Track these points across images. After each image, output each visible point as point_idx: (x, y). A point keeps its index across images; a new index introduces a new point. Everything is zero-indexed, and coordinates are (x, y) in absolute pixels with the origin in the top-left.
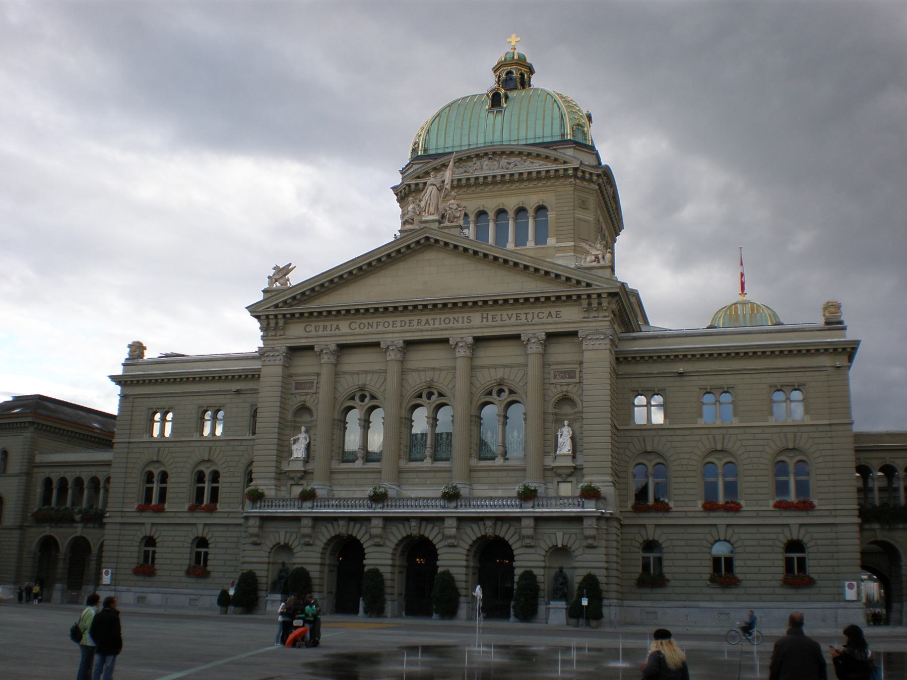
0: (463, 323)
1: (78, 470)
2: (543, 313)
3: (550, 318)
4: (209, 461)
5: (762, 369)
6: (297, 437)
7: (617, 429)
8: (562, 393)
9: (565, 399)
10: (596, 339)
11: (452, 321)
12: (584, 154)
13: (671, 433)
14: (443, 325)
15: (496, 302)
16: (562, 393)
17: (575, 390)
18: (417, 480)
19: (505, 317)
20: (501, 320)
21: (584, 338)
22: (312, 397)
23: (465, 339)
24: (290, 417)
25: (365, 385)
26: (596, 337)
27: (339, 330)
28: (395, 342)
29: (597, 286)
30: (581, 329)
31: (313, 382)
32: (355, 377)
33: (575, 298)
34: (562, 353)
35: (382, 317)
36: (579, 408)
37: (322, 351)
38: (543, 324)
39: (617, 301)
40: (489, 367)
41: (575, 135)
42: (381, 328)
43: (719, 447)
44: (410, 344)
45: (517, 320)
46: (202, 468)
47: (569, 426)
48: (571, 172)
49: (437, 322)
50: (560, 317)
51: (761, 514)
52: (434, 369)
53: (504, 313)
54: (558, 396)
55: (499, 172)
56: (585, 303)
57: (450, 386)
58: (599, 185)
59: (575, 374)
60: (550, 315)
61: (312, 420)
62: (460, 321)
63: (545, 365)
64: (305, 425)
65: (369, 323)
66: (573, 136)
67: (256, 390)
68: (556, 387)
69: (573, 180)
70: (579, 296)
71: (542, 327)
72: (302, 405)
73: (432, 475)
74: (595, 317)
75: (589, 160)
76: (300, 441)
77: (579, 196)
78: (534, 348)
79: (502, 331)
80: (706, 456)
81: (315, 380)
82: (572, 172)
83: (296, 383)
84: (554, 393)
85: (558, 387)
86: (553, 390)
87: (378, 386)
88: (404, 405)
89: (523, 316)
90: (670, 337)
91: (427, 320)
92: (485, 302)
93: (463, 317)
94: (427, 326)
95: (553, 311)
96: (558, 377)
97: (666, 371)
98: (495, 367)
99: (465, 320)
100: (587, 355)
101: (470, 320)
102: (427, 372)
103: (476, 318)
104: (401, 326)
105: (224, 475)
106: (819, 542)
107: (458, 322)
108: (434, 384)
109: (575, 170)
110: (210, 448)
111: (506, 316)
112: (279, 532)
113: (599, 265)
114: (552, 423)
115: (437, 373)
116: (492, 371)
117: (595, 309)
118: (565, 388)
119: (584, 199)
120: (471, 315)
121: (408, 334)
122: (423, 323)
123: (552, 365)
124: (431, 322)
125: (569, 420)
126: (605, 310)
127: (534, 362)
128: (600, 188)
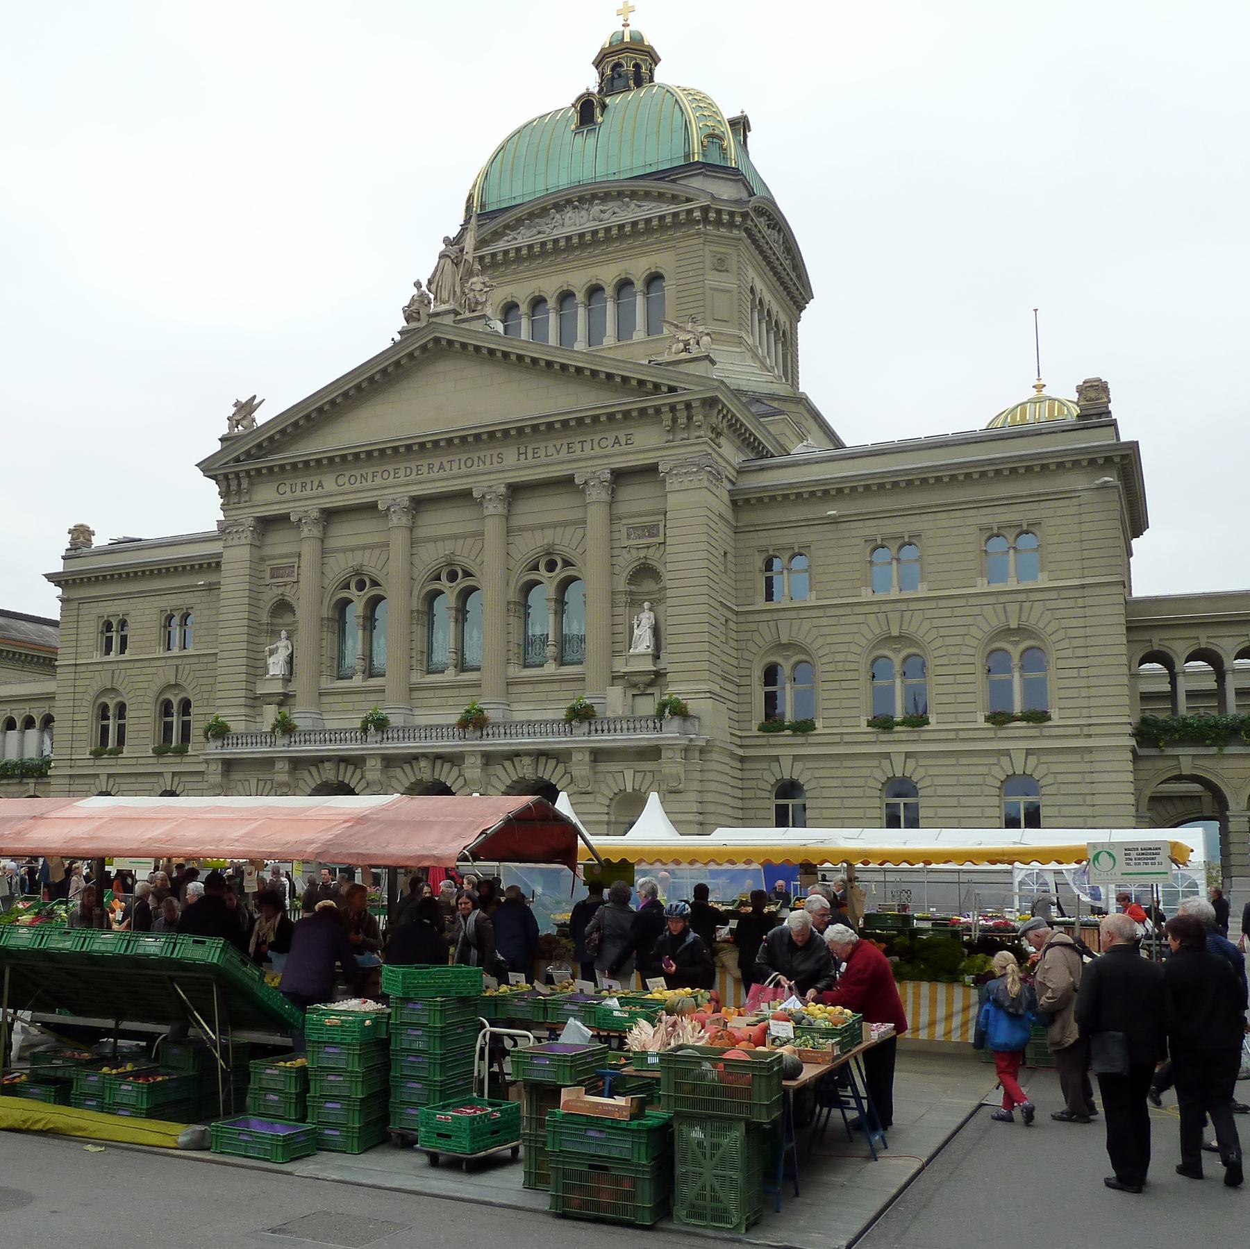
0: (492, 464)
1: (26, 706)
4: (176, 685)
5: (963, 503)
6: (275, 646)
7: (737, 613)
8: (638, 560)
9: (645, 572)
10: (685, 473)
11: (476, 463)
12: (721, 183)
13: (820, 613)
14: (464, 469)
15: (535, 428)
16: (638, 560)
17: (658, 555)
19: (551, 451)
21: (667, 473)
24: (265, 618)
25: (362, 566)
26: (685, 471)
28: (398, 500)
30: (661, 459)
32: (349, 555)
33: (651, 411)
34: (636, 498)
37: (300, 520)
38: (606, 456)
39: (719, 412)
40: (533, 528)
41: (707, 153)
42: (378, 481)
43: (895, 633)
44: (419, 503)
46: (168, 696)
48: (697, 214)
49: (455, 466)
51: (962, 735)
52: (455, 537)
53: (550, 444)
54: (633, 565)
55: (592, 225)
56: (667, 418)
57: (478, 560)
58: (747, 230)
60: (617, 441)
62: (488, 460)
63: (613, 519)
64: (287, 629)
66: (704, 155)
67: (215, 584)
68: (629, 551)
69: (701, 226)
70: (658, 410)
71: (605, 461)
72: (280, 600)
74: (683, 439)
75: (726, 191)
76: (279, 651)
77: (710, 251)
78: (597, 494)
80: (875, 647)
82: (699, 214)
83: (271, 569)
84: (626, 562)
85: (634, 552)
87: (379, 567)
88: (416, 592)
89: (578, 447)
90: (817, 463)
91: (441, 463)
92: (520, 430)
93: (492, 455)
97: (810, 516)
98: (542, 527)
99: (495, 459)
100: (673, 500)
101: (502, 459)
103: (510, 456)
105: (198, 704)
106: (1060, 778)
108: (456, 558)
109: (705, 210)
110: (177, 666)
113: (688, 356)
114: (625, 606)
115: (460, 542)
116: (538, 533)
117: (683, 426)
118: (642, 554)
119: (722, 256)
120: (500, 450)
121: (415, 487)
122: (436, 469)
123: (625, 518)
124: (447, 466)
125: (652, 602)
126: (699, 426)
127: (596, 515)
128: (750, 235)
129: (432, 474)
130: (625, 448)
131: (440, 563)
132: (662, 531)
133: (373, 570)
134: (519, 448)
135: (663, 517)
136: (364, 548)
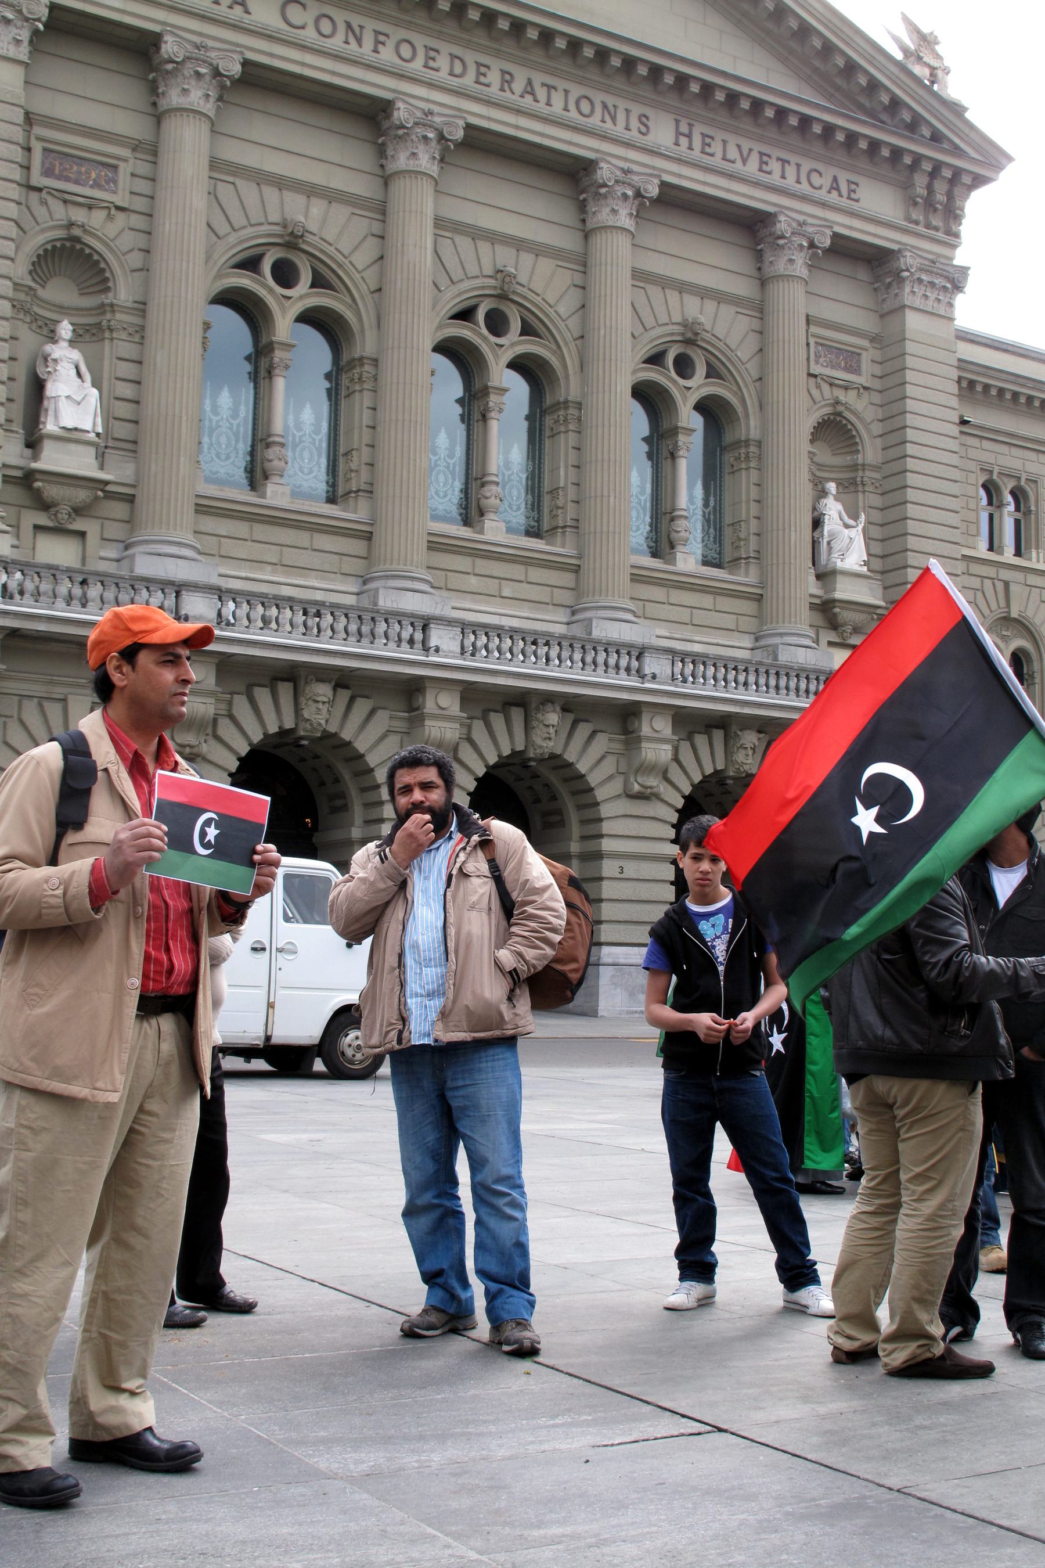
0: (627, 128)
2: (820, 174)
3: (835, 193)
10: (932, 284)
18: (473, 580)
19: (733, 153)
20: (724, 159)
22: (110, 217)
23: (635, 178)
27: (248, 12)
29: (956, 147)
31: (115, 168)
32: (271, 194)
33: (908, 160)
35: (398, 23)
36: (870, 452)
42: (387, 55)
45: (761, 170)
47: (836, 499)
49: (558, 100)
50: (857, 201)
52: (519, 244)
53: (732, 140)
56: (920, 181)
59: (859, 361)
61: (103, 305)
62: (621, 116)
65: (349, 26)
73: (516, 571)
79: (728, 191)
81: (125, 160)
85: (825, 387)
86: (815, 392)
89: (775, 166)
91: (530, 82)
94: (529, 98)
95: (843, 177)
96: (821, 360)
102: (499, 248)
104: (451, 74)
107: (614, 119)
108: (519, 290)
111: (736, 149)
112: (64, 700)
116: (673, 296)
120: (648, 111)
122: (518, 86)
124: (541, 93)
125: (839, 484)
129: (508, 94)
130: (844, 199)
131: (483, 288)
132: (866, 365)
133: (331, 250)
134: (677, 121)
135: (865, 343)
136: (310, 191)
